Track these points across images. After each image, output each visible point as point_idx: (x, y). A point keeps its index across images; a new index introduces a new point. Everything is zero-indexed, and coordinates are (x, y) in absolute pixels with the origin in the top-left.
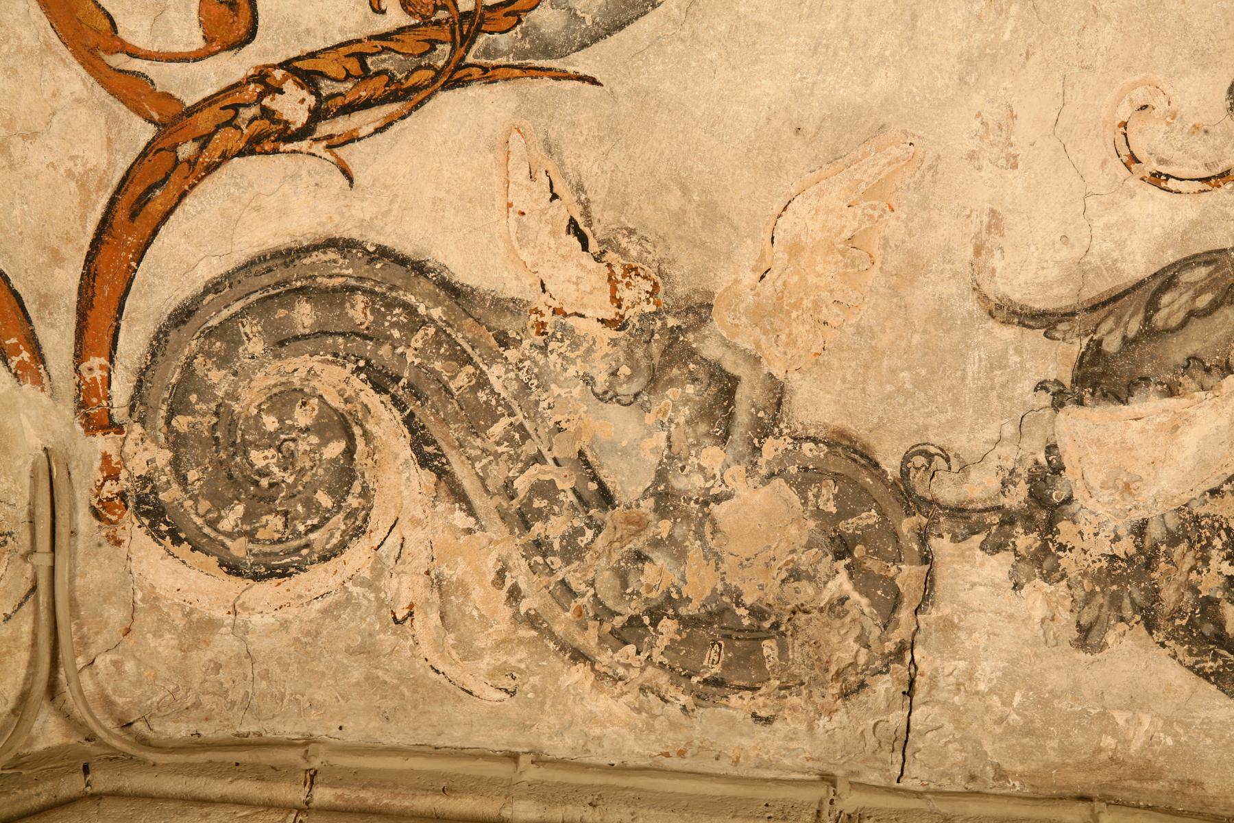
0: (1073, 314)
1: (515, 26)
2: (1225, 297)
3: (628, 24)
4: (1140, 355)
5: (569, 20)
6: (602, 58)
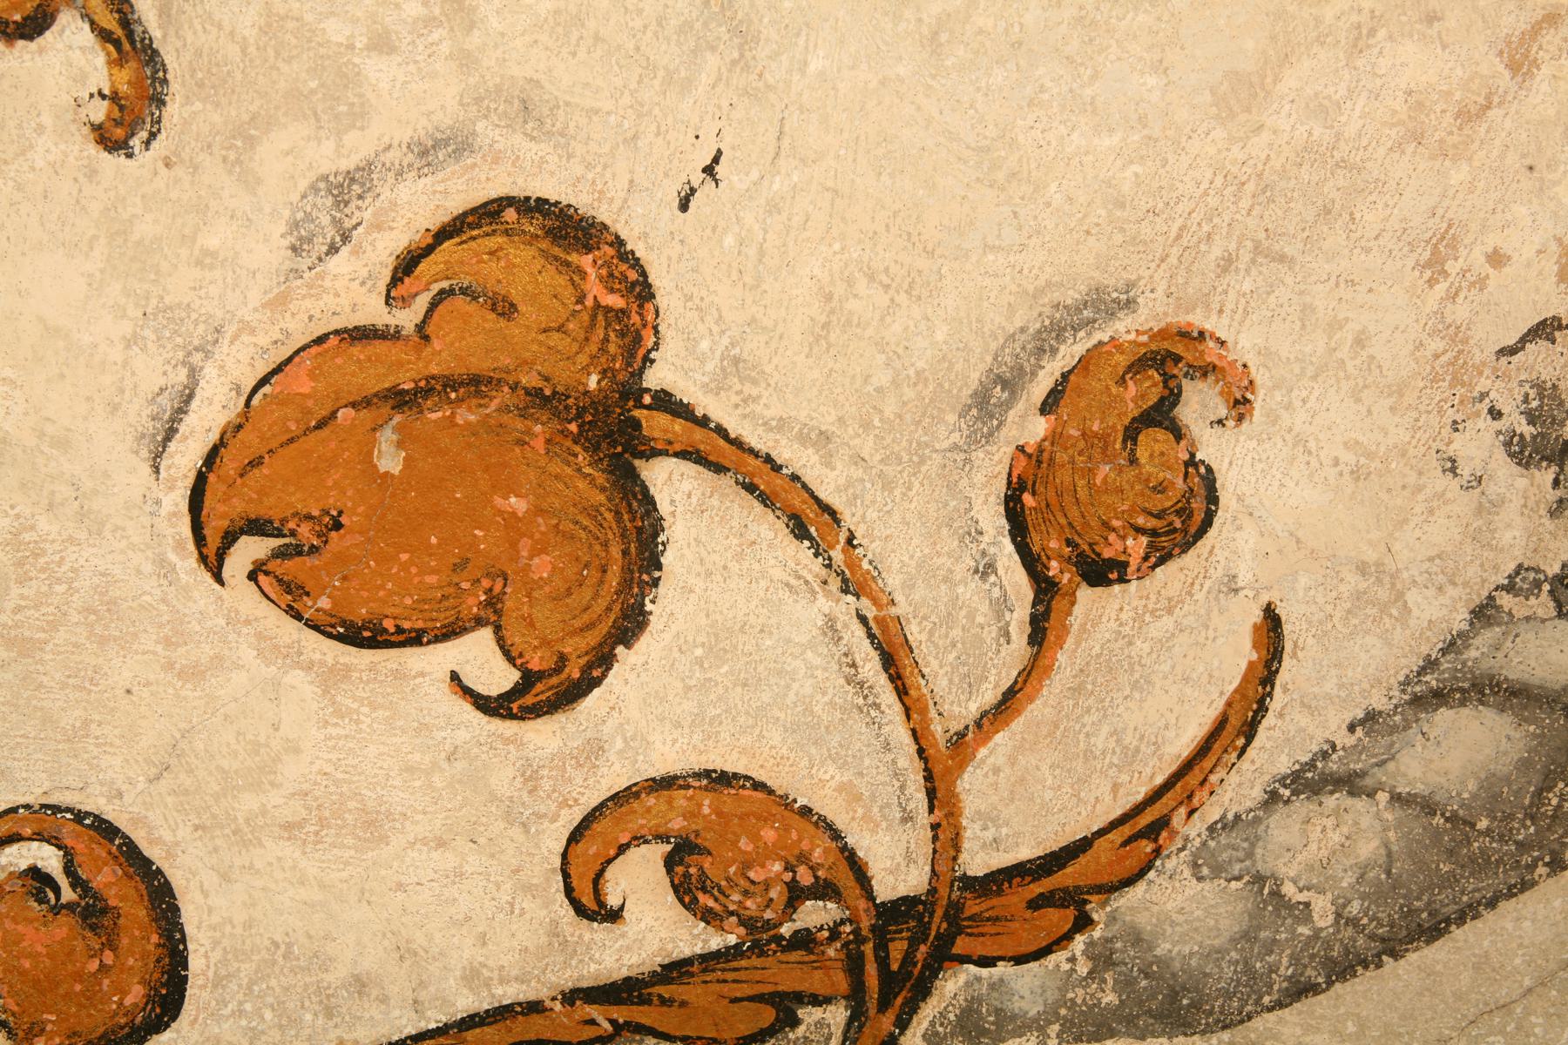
1: (1068, 937)
3: (1461, 920)
5: (1255, 915)
6: (1362, 1026)
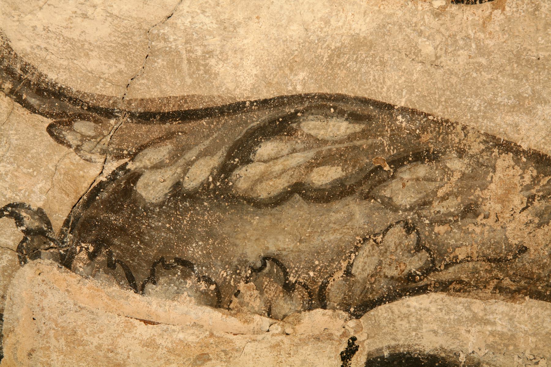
0: (109, 113)
2: (359, 184)
4: (193, 223)
